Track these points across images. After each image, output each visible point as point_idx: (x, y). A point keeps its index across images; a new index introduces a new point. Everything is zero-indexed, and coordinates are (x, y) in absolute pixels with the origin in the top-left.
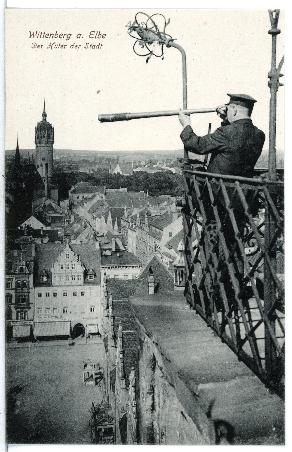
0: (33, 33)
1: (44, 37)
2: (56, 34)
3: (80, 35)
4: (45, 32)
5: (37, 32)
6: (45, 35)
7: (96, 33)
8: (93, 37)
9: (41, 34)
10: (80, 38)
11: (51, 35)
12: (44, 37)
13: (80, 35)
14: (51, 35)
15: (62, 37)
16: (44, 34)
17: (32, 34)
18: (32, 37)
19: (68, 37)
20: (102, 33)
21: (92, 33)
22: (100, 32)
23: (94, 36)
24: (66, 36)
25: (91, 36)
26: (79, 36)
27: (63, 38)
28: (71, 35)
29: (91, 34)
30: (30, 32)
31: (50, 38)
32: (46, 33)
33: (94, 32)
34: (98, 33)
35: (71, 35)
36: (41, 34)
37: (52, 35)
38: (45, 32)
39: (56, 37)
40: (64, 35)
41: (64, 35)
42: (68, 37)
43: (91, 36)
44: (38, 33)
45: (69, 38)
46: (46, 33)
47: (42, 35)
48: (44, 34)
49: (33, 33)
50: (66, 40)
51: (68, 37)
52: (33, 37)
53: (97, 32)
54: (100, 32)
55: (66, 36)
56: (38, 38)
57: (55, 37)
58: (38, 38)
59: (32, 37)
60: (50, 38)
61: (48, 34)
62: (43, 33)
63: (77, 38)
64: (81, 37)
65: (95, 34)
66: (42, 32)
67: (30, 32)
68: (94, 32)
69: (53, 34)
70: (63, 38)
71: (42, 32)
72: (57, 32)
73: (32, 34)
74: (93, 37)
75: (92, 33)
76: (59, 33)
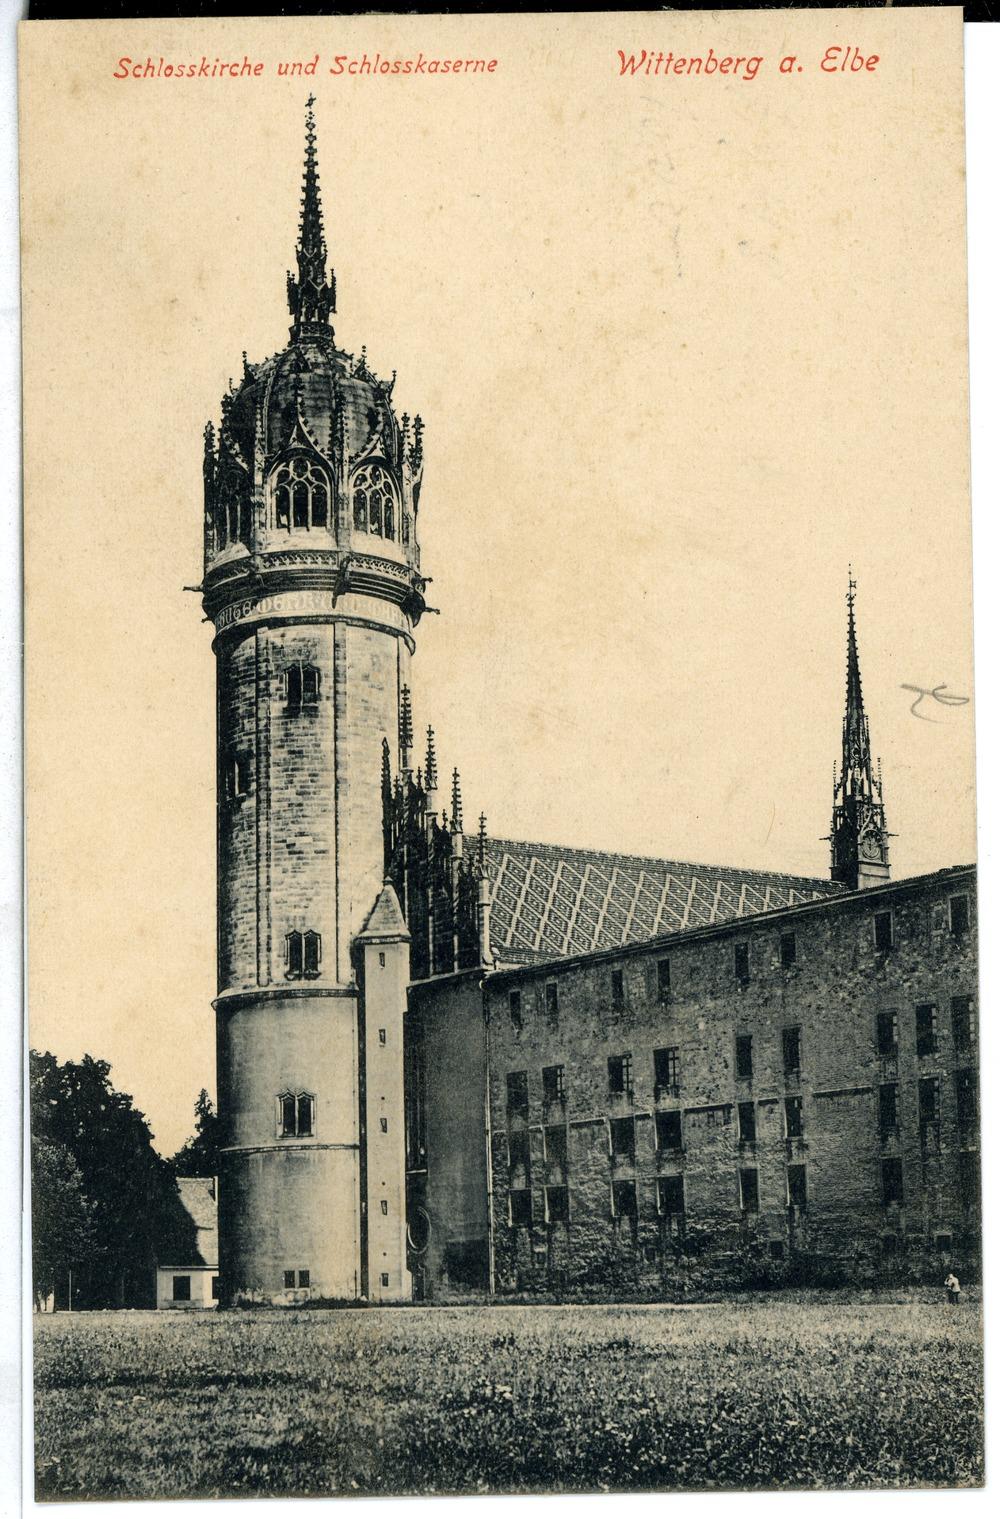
0: (632, 60)
3: (792, 60)
4: (671, 55)
5: (644, 54)
7: (845, 50)
8: (834, 69)
9: (660, 60)
10: (790, 70)
11: (693, 61)
13: (792, 60)
14: (693, 61)
18: (629, 69)
19: (752, 67)
21: (832, 53)
22: (857, 49)
23: (837, 63)
25: (829, 64)
26: (787, 65)
28: (759, 60)
29: (828, 58)
30: (621, 53)
33: (839, 49)
34: (852, 53)
35: (759, 60)
36: (660, 60)
38: (671, 55)
40: (738, 61)
41: (738, 61)
42: (752, 66)
43: (829, 64)
44: (648, 57)
45: (755, 72)
46: (676, 57)
47: (664, 64)
48: (669, 60)
49: (632, 60)
50: (745, 78)
52: (633, 71)
53: (849, 49)
54: (857, 49)
56: (647, 72)
57: (707, 71)
58: (647, 72)
59: (629, 69)
61: (684, 61)
63: (782, 70)
65: (841, 56)
66: (661, 55)
67: (621, 53)
68: (839, 49)
70: (735, 71)
71: (661, 55)
72: (711, 51)
74: (834, 69)
76: (720, 56)
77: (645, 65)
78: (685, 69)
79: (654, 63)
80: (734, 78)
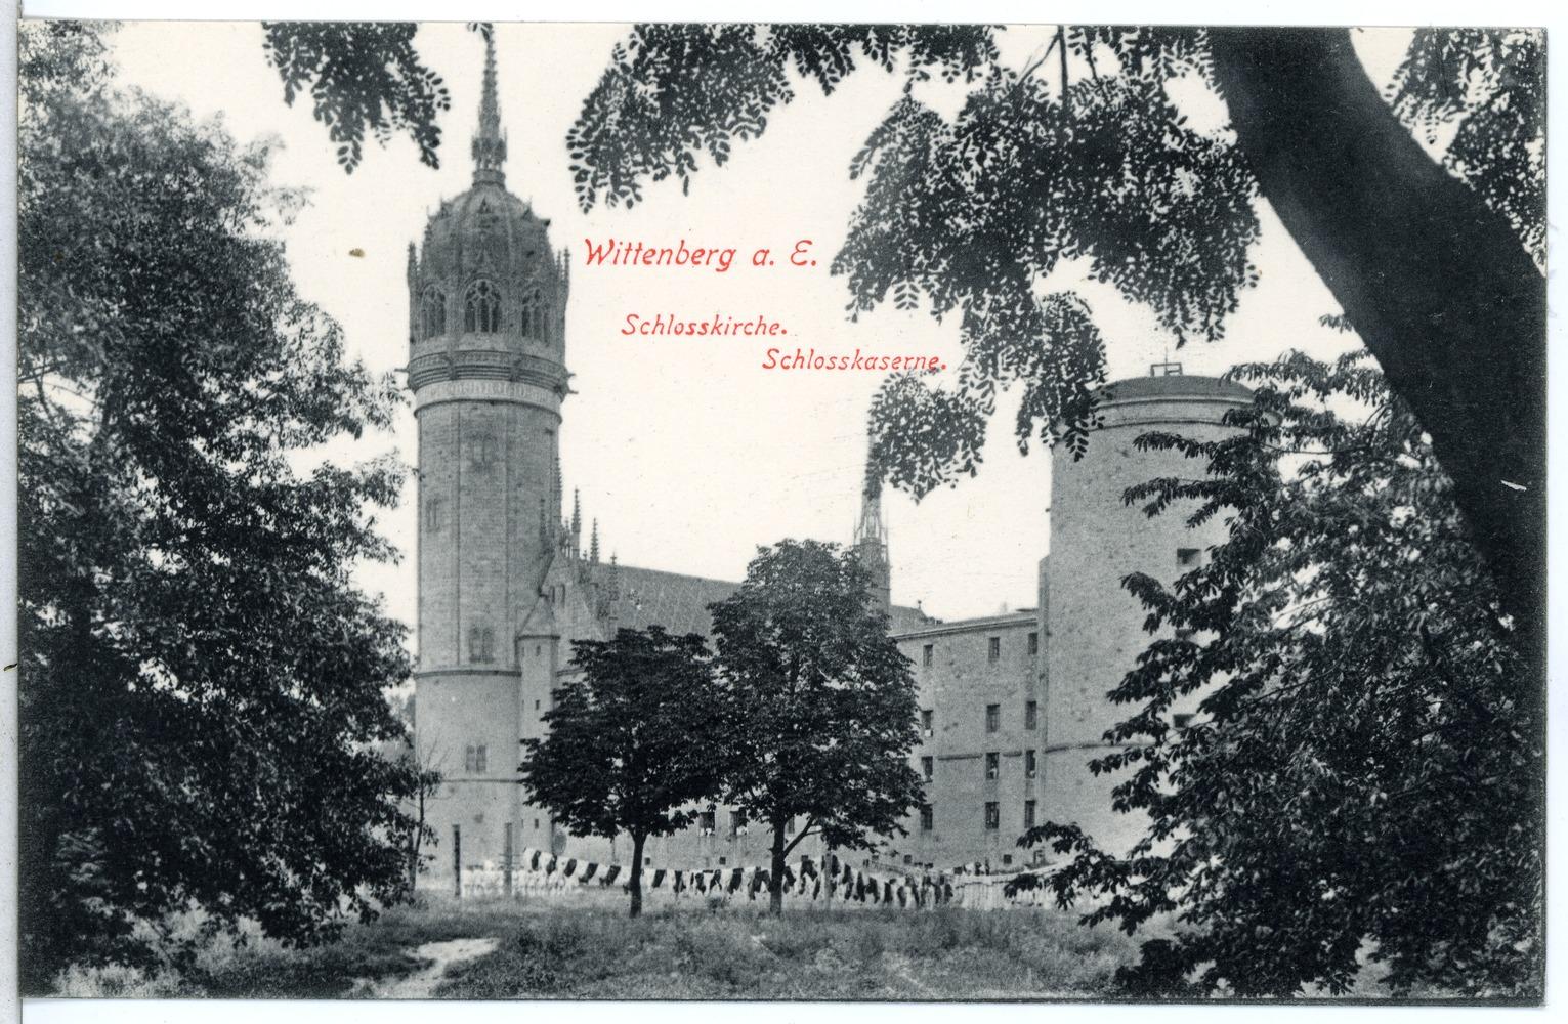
0: (600, 249)
1: (640, 259)
3: (766, 252)
5: (612, 242)
6: (641, 254)
8: (804, 263)
9: (628, 250)
10: (763, 263)
11: (663, 252)
12: (640, 259)
13: (766, 252)
14: (663, 252)
15: (703, 260)
17: (594, 249)
18: (596, 258)
19: (725, 260)
21: (803, 246)
24: (715, 258)
25: (799, 258)
26: (760, 258)
28: (732, 253)
30: (588, 241)
32: (646, 248)
35: (732, 253)
36: (628, 250)
37: (667, 255)
39: (681, 259)
42: (726, 259)
43: (799, 258)
44: (617, 246)
46: (646, 248)
47: (632, 254)
49: (600, 249)
51: (725, 260)
52: (601, 259)
55: (715, 258)
57: (678, 262)
59: (596, 258)
62: (635, 246)
63: (755, 263)
64: (768, 261)
67: (588, 241)
73: (594, 249)
74: (804, 263)
75: (801, 247)
76: (692, 247)
77: (613, 254)
78: (654, 259)
79: (623, 253)
80: (707, 271)
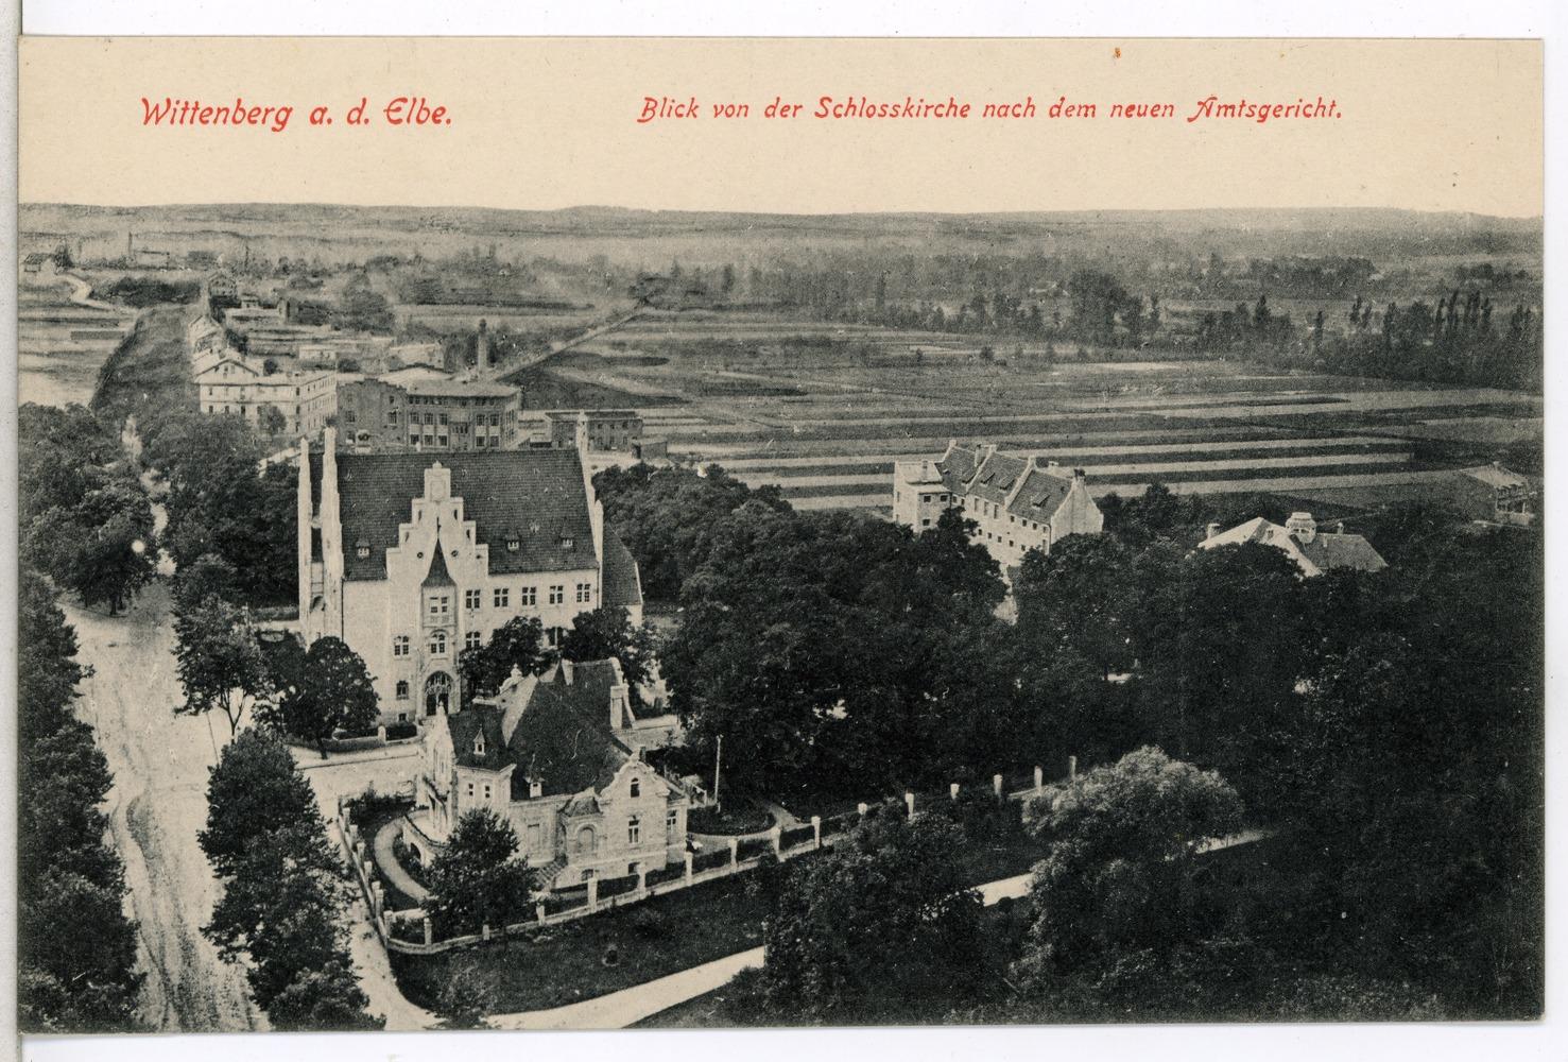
1: (197, 118)
2: (238, 108)
7: (410, 103)
9: (185, 109)
11: (219, 111)
12: (197, 118)
14: (219, 111)
16: (196, 109)
20: (432, 106)
22: (423, 100)
24: (272, 116)
27: (264, 121)
31: (215, 121)
36: (185, 109)
38: (197, 103)
40: (267, 111)
42: (282, 116)
44: (173, 105)
45: (283, 124)
47: (189, 113)
53: (415, 100)
54: (423, 100)
60: (215, 121)
61: (210, 110)
65: (406, 107)
66: (187, 103)
69: (227, 110)
70: (264, 121)
71: (187, 103)
72: (239, 101)
76: (248, 107)
